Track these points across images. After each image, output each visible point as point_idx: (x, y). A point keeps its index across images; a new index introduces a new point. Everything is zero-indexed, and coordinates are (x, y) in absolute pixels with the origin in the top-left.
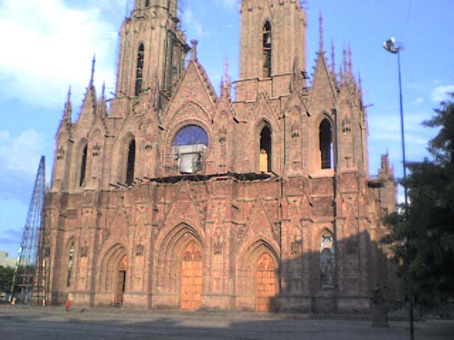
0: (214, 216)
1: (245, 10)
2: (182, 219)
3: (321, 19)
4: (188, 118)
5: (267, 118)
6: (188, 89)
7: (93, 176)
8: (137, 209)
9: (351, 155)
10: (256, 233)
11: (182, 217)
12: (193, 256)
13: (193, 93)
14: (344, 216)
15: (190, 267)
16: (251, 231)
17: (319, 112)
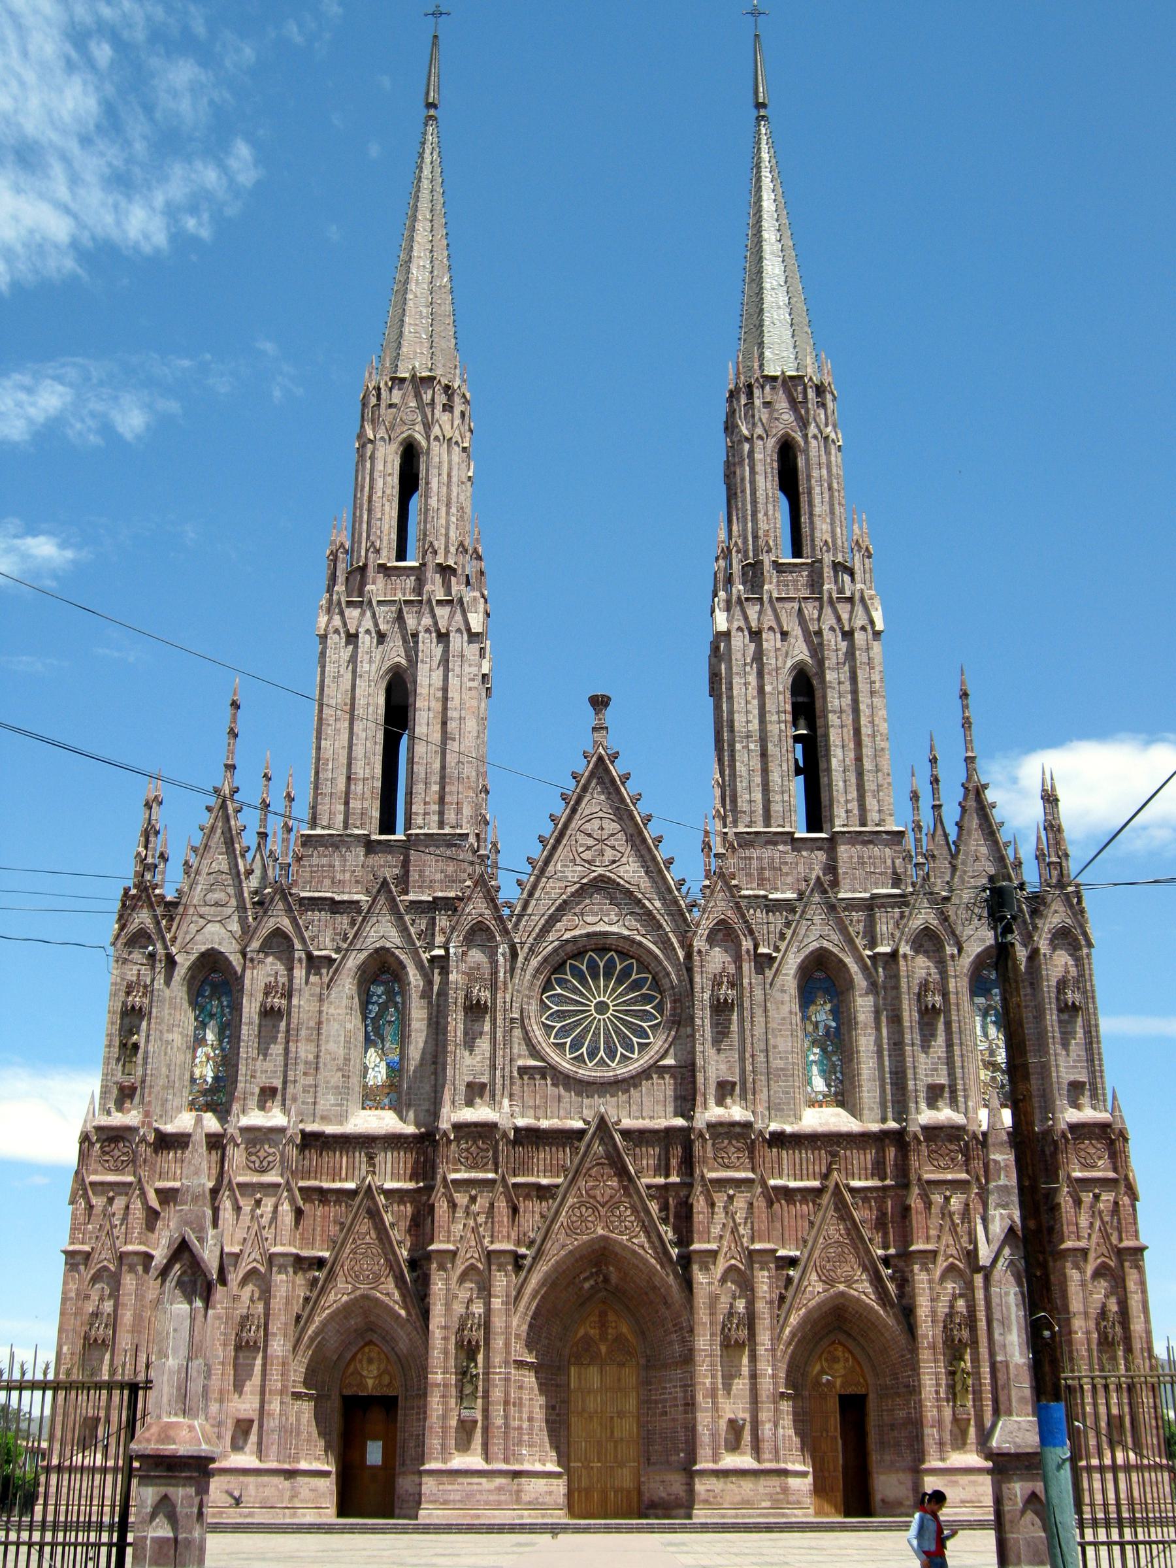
0: (716, 1230)
1: (740, 629)
2: (603, 1238)
3: (965, 695)
4: (597, 929)
5: (835, 950)
6: (591, 842)
7: (262, 1080)
8: (453, 1206)
9: (1083, 1078)
10: (830, 1282)
11: (600, 1231)
12: (603, 1349)
13: (609, 854)
14: (1082, 1244)
15: (596, 1384)
16: (814, 1277)
17: (979, 950)
